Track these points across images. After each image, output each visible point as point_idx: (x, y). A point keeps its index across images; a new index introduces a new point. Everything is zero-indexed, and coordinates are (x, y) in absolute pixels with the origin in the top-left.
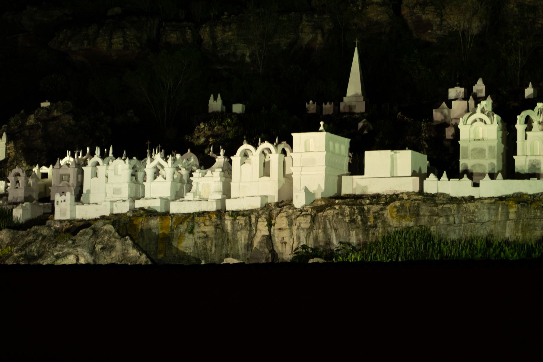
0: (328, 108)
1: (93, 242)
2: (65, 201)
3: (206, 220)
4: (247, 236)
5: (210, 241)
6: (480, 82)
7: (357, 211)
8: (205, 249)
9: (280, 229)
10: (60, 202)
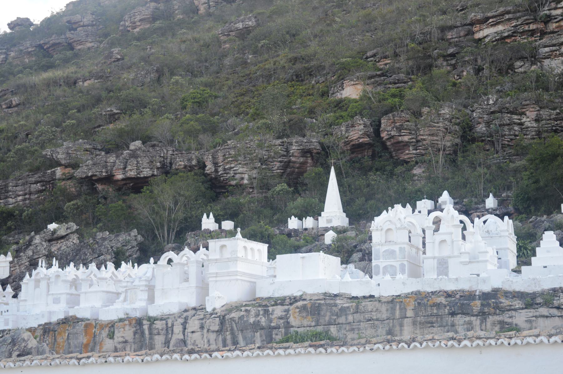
0: (309, 222)
1: (10, 350)
2: (8, 311)
3: (125, 325)
4: (164, 340)
5: (129, 346)
6: (445, 193)
7: (261, 313)
9: (193, 332)
10: (3, 312)
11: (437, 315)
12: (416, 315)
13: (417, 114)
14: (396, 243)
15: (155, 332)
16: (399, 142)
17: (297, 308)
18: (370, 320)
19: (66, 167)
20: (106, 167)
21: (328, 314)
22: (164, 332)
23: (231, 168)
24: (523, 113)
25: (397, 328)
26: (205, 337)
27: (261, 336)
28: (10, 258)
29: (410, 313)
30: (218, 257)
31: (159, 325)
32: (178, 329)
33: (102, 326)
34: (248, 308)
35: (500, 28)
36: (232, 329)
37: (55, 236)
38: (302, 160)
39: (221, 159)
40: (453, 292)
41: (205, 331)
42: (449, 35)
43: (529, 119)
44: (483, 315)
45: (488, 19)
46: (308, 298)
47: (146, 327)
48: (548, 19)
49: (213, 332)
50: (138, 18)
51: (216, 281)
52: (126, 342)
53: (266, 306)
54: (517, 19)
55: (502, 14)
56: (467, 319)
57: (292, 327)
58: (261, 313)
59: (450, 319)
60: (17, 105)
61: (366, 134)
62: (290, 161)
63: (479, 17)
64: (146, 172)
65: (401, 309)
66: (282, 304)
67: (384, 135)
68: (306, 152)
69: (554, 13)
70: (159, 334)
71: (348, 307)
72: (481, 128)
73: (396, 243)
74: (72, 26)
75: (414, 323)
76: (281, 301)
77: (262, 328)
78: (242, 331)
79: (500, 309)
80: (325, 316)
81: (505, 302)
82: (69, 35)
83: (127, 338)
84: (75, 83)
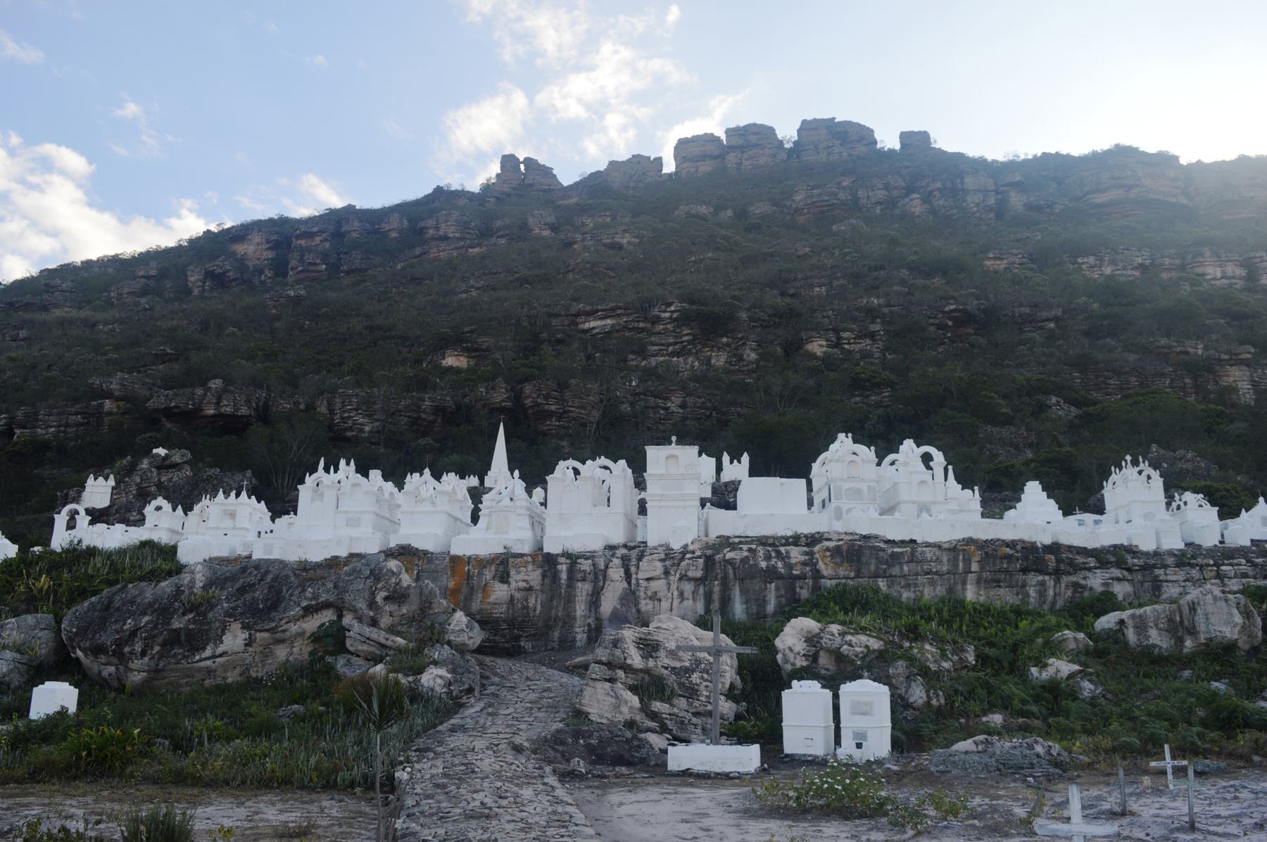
8: (526, 608)
9: (648, 579)
11: (1006, 571)
12: (982, 569)
13: (562, 386)
14: (863, 480)
15: (579, 576)
16: (544, 411)
17: (828, 549)
18: (927, 573)
19: (118, 399)
20: (193, 399)
21: (873, 561)
22: (590, 577)
23: (350, 417)
24: (666, 399)
25: (959, 587)
26: (674, 587)
27: (777, 589)
28: (112, 482)
29: (975, 567)
30: (663, 471)
31: (585, 565)
32: (616, 573)
33: (482, 563)
34: (754, 547)
35: (609, 321)
36: (725, 577)
37: (168, 462)
38: (432, 418)
39: (338, 405)
40: (1013, 541)
41: (674, 578)
42: (555, 322)
43: (674, 404)
44: (1057, 573)
45: (597, 311)
46: (835, 537)
47: (563, 568)
48: (657, 320)
49: (690, 579)
50: (126, 290)
51: (660, 507)
52: (530, 589)
53: (773, 545)
54: (628, 315)
55: (613, 309)
56: (1040, 578)
57: (824, 577)
58: (773, 554)
59: (1021, 577)
60: (24, 339)
61: (509, 398)
62: (420, 418)
63: (588, 308)
64: (244, 411)
65: (964, 560)
66: (796, 544)
67: (528, 402)
68: (438, 410)
69: (663, 315)
70: (584, 580)
71: (902, 553)
72: (626, 408)
73: (863, 480)
74: (49, 288)
75: (978, 582)
76: (795, 540)
77: (780, 577)
78: (742, 580)
79: (1076, 568)
80: (868, 564)
81: (1080, 559)
82: (46, 296)
83: (532, 583)
84: (94, 325)
